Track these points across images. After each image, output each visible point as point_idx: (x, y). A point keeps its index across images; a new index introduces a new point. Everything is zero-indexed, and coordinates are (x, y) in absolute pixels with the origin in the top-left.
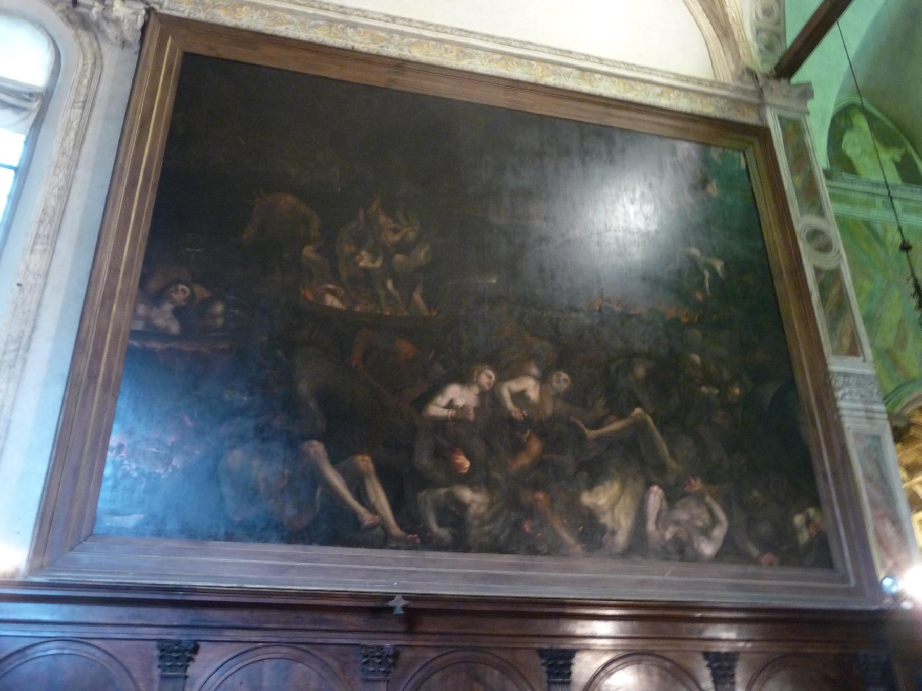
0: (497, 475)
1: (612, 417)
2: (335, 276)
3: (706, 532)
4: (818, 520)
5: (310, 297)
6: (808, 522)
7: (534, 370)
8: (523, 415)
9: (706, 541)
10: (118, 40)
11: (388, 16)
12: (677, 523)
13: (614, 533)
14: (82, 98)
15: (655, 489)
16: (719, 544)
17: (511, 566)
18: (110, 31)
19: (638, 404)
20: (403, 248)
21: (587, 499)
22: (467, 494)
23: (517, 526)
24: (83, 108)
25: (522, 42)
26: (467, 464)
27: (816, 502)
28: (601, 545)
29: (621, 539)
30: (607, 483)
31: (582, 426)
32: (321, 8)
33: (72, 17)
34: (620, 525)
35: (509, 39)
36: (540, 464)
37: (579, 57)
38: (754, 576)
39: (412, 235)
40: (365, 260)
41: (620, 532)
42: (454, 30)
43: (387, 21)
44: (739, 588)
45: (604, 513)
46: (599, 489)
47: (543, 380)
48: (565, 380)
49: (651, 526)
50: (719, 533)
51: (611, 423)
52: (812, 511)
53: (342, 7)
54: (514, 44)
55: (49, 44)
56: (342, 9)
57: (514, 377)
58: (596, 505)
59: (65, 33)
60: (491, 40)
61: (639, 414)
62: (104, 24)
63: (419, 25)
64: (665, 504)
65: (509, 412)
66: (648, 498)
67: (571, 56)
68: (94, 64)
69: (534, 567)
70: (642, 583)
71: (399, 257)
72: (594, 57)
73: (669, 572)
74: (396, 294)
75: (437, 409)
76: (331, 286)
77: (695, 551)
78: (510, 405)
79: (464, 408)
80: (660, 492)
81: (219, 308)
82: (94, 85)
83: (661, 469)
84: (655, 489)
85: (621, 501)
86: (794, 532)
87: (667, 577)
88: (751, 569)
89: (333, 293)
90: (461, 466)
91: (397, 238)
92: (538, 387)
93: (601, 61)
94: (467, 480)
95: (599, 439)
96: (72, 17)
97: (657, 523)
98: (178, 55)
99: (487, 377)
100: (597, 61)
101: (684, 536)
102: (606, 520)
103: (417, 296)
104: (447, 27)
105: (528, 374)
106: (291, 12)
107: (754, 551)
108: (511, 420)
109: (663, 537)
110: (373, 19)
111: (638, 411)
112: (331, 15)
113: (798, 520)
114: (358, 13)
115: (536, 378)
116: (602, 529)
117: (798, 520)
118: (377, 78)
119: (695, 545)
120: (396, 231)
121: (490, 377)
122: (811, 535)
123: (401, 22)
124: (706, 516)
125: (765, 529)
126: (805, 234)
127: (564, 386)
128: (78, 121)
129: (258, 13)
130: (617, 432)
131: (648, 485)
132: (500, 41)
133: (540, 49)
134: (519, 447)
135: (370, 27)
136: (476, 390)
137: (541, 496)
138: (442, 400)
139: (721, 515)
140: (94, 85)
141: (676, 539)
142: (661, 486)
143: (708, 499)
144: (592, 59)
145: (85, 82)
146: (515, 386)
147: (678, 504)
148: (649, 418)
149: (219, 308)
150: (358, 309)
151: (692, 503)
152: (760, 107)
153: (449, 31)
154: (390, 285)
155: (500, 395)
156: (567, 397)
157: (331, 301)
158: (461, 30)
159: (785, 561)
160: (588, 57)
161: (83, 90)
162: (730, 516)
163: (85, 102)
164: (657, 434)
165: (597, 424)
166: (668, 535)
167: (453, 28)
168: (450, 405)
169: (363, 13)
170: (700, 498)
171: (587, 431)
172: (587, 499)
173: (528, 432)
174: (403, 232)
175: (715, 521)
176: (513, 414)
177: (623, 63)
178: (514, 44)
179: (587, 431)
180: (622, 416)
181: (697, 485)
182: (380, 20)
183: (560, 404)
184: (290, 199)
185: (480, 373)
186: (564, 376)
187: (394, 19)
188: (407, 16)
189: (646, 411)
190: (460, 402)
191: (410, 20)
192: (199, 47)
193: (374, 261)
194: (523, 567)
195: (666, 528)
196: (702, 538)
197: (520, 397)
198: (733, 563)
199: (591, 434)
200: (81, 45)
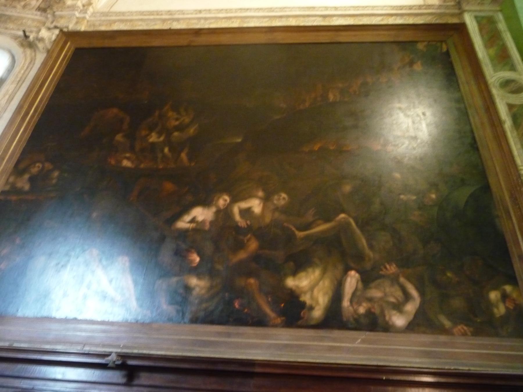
0: (219, 267)
1: (320, 222)
2: (132, 149)
3: (398, 307)
4: (515, 295)
5: (113, 162)
6: (505, 297)
7: (261, 194)
8: (247, 224)
9: (398, 314)
10: (44, 50)
11: (196, 10)
12: (370, 300)
13: (311, 308)
14: (18, 79)
15: (353, 273)
16: (411, 317)
17: (219, 334)
18: (40, 45)
19: (343, 211)
20: (180, 128)
21: (290, 282)
22: (194, 281)
23: (230, 303)
24: (18, 84)
26: (198, 259)
27: (513, 280)
28: (299, 318)
29: (318, 313)
30: (310, 270)
31: (294, 229)
33: (24, 43)
34: (317, 303)
36: (256, 258)
38: (445, 344)
39: (187, 120)
40: (153, 138)
41: (317, 308)
42: (236, 10)
44: (427, 354)
45: (305, 293)
46: (302, 274)
47: (266, 199)
48: (284, 198)
49: (346, 303)
50: (411, 308)
51: (318, 225)
52: (508, 288)
55: (9, 58)
56: (169, 12)
57: (244, 199)
58: (297, 287)
59: (18, 50)
61: (344, 218)
62: (37, 42)
64: (360, 285)
65: (237, 223)
66: (345, 280)
68: (30, 63)
69: (238, 335)
70: (331, 349)
71: (176, 134)
73: (359, 341)
74: (170, 155)
75: (183, 224)
76: (128, 155)
77: (387, 323)
78: (237, 217)
79: (203, 222)
80: (357, 275)
81: (56, 174)
82: (27, 73)
83: (360, 257)
84: (353, 273)
85: (321, 283)
86: (490, 305)
87: (357, 344)
88: (443, 338)
89: (128, 159)
90: (192, 261)
91: (177, 123)
92: (262, 205)
94: (196, 271)
95: (307, 238)
96: (24, 43)
97: (351, 301)
98: (73, 49)
99: (223, 201)
101: (377, 310)
102: (306, 298)
103: (183, 155)
105: (256, 197)
106: (142, 20)
107: (447, 323)
108: (237, 229)
109: (355, 311)
111: (342, 216)
112: (164, 17)
113: (494, 295)
115: (260, 198)
116: (302, 305)
117: (494, 295)
118: (183, 41)
119: (387, 318)
120: (177, 119)
121: (226, 200)
122: (507, 308)
124: (399, 294)
125: (457, 303)
126: (498, 84)
127: (282, 202)
128: (12, 90)
129: (124, 24)
130: (323, 232)
131: (347, 270)
134: (240, 246)
135: (186, 19)
136: (214, 209)
137: (252, 281)
138: (187, 218)
139: (414, 292)
140: (27, 73)
141: (369, 313)
142: (358, 271)
143: (402, 280)
145: (22, 72)
146: (244, 205)
147: (373, 285)
148: (352, 221)
149: (56, 174)
150: (142, 166)
151: (387, 283)
152: (460, 14)
154: (166, 150)
155: (232, 211)
156: (285, 210)
157: (126, 163)
159: (477, 332)
161: (20, 75)
162: (422, 294)
163: (19, 81)
164: (358, 231)
165: (308, 227)
166: (362, 310)
168: (193, 221)
169: (182, 12)
170: (394, 280)
171: (297, 232)
172: (290, 282)
173: (249, 236)
174: (182, 119)
175: (407, 297)
176: (239, 224)
179: (297, 232)
180: (327, 220)
181: (392, 269)
183: (277, 215)
184: (115, 111)
185: (219, 198)
186: (284, 195)
187: (200, 12)
188: (208, 8)
189: (349, 215)
190: (200, 218)
191: (209, 10)
192: (84, 44)
193: (159, 137)
194: (229, 335)
195: (359, 304)
196: (394, 312)
197: (246, 213)
198: (424, 333)
199: (300, 234)
200: (25, 55)
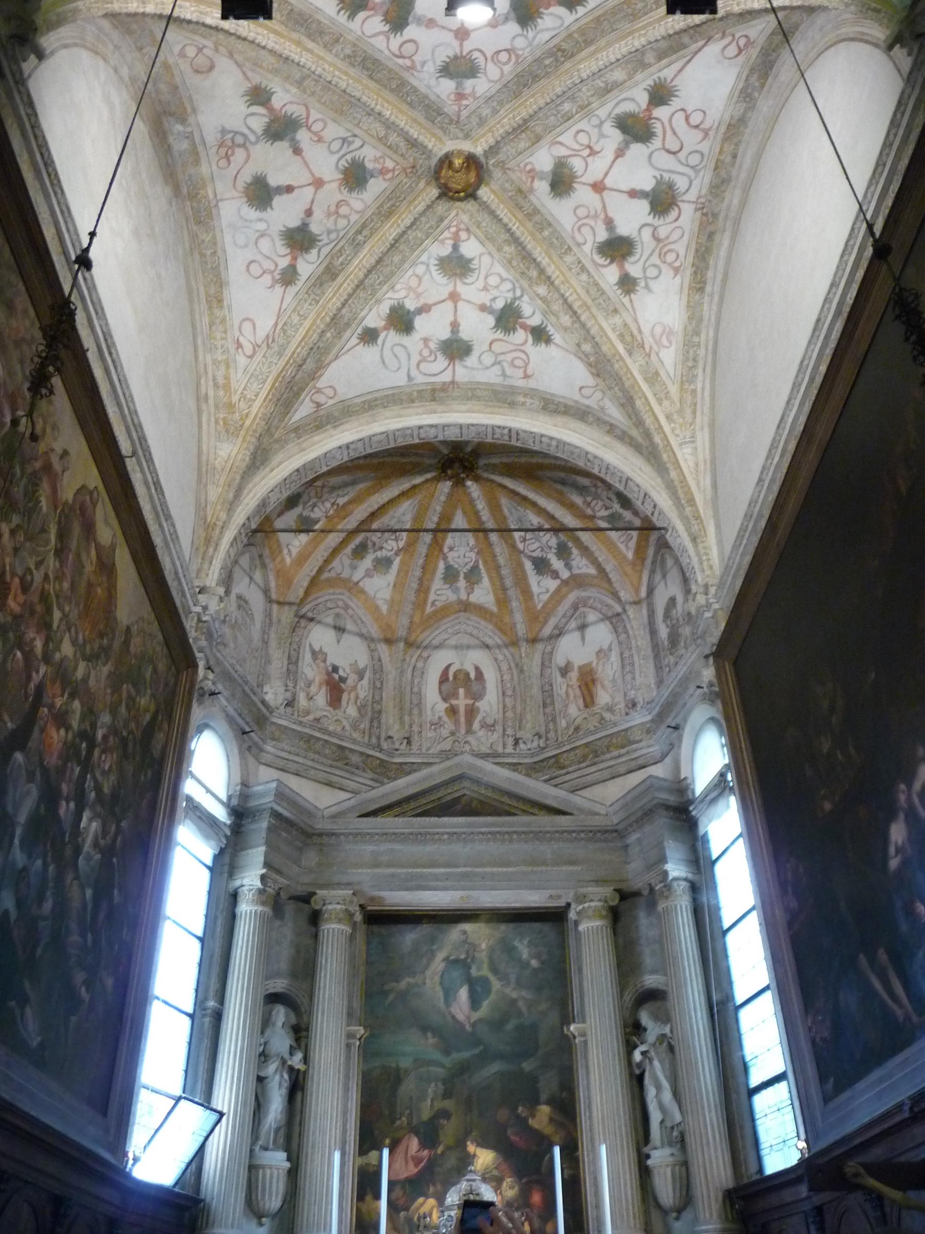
11: (758, 483)
25: (799, 370)
32: (745, 531)
35: (794, 383)
37: (825, 310)
43: (763, 486)
53: (746, 515)
54: (800, 379)
60: (792, 401)
63: (769, 461)
67: (823, 320)
72: (829, 293)
93: (833, 285)
100: (834, 290)
104: (774, 438)
110: (759, 496)
114: (752, 505)
123: (764, 475)
132: (795, 392)
133: (809, 353)
144: (831, 295)
153: (778, 438)
158: (778, 427)
160: (827, 300)
167: (776, 433)
177: (842, 256)
178: (800, 379)
182: (760, 492)
188: (760, 469)
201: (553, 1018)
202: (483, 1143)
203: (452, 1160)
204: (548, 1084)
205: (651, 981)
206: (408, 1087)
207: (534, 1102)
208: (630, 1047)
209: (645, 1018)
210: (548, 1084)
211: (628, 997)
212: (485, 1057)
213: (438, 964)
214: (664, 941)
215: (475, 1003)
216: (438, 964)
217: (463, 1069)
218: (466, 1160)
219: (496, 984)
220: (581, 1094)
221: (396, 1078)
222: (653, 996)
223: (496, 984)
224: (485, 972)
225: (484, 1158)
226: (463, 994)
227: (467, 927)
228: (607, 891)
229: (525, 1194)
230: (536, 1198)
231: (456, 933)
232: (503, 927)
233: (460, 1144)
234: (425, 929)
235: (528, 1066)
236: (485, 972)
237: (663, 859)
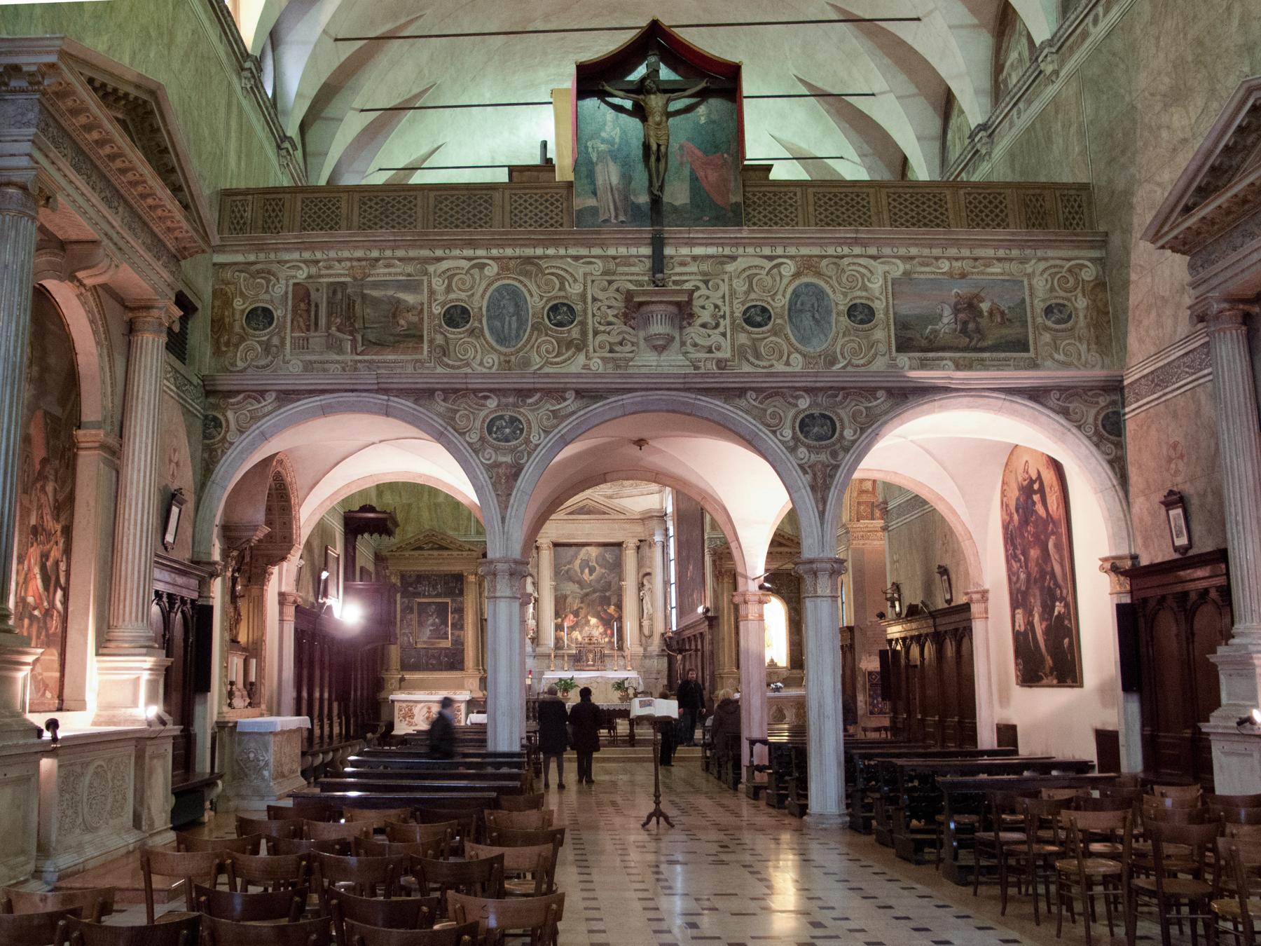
201: (617, 579)
202: (593, 616)
203: (583, 621)
204: (614, 600)
205: (648, 570)
206: (569, 600)
207: (609, 605)
208: (640, 590)
209: (645, 582)
210: (614, 600)
211: (641, 574)
212: (594, 591)
213: (578, 562)
214: (651, 558)
215: (591, 574)
216: (578, 562)
217: (587, 595)
218: (588, 622)
219: (598, 568)
220: (624, 604)
221: (566, 597)
222: (649, 574)
223: (598, 568)
224: (594, 564)
225: (593, 621)
226: (587, 571)
227: (589, 548)
228: (636, 540)
229: (605, 631)
230: (609, 632)
231: (584, 550)
232: (601, 548)
233: (586, 616)
234: (573, 550)
235: (607, 594)
236: (594, 564)
237: (654, 535)
